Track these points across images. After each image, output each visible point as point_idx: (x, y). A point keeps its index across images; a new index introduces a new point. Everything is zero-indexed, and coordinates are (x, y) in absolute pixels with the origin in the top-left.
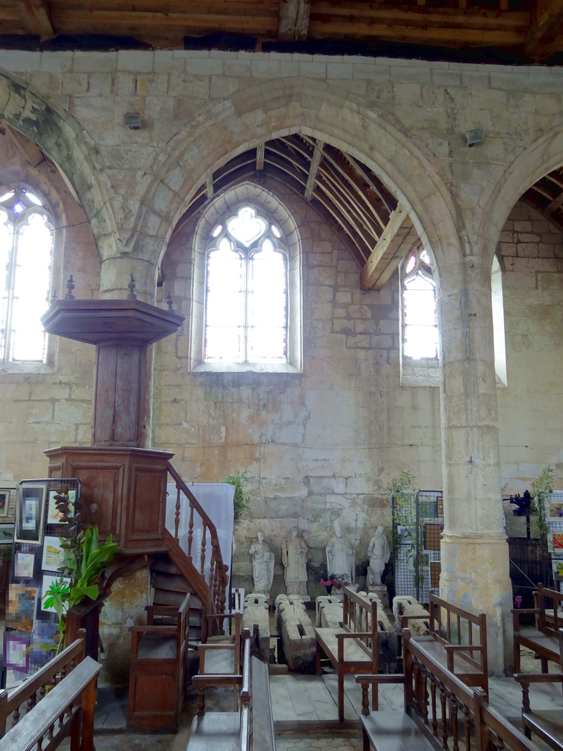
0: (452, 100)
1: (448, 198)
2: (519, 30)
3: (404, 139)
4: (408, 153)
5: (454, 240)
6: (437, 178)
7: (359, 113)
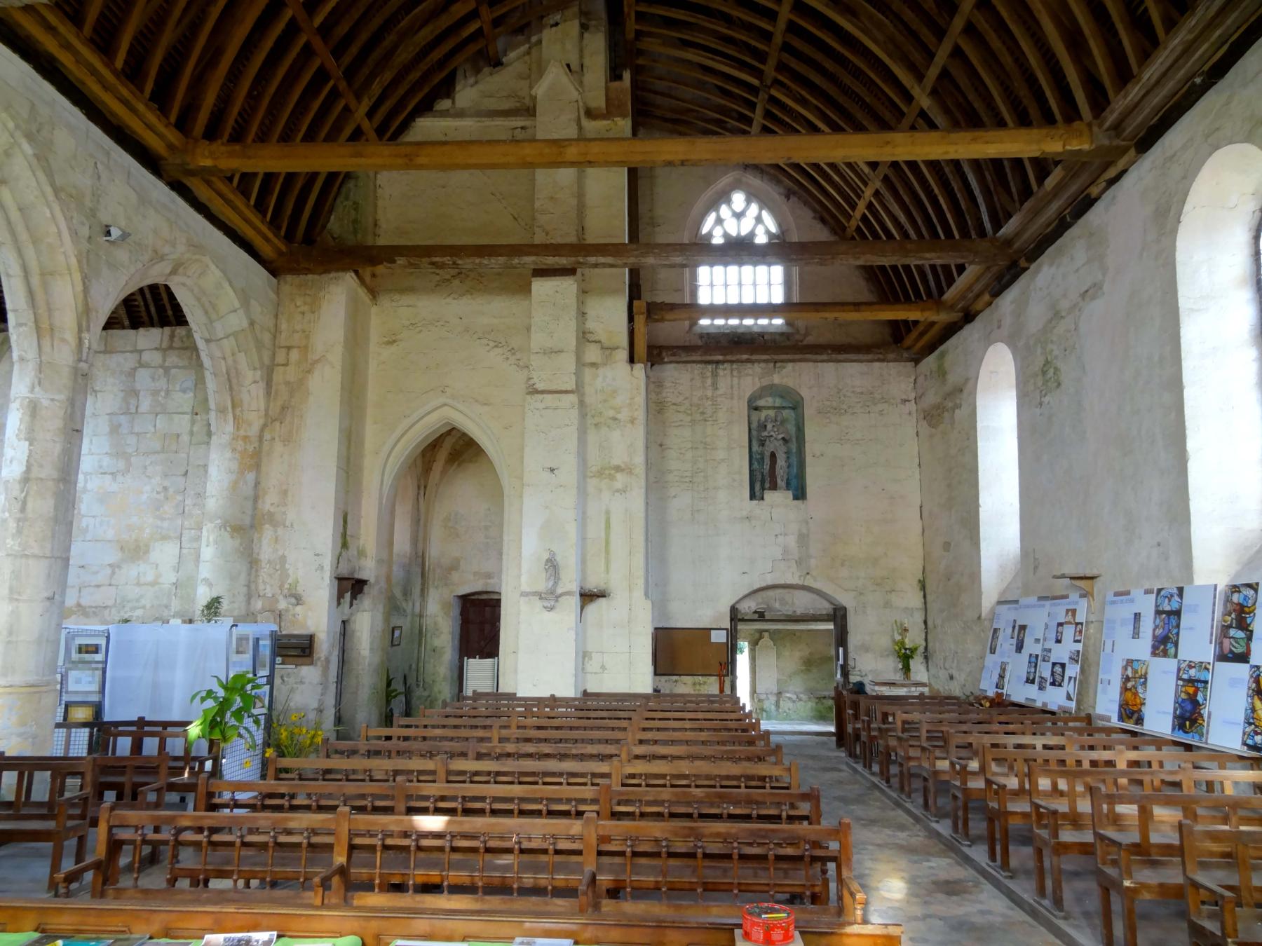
0: (99, 177)
1: (79, 288)
2: (171, 147)
3: (51, 197)
4: (48, 215)
5: (70, 337)
6: (73, 261)
7: (12, 136)
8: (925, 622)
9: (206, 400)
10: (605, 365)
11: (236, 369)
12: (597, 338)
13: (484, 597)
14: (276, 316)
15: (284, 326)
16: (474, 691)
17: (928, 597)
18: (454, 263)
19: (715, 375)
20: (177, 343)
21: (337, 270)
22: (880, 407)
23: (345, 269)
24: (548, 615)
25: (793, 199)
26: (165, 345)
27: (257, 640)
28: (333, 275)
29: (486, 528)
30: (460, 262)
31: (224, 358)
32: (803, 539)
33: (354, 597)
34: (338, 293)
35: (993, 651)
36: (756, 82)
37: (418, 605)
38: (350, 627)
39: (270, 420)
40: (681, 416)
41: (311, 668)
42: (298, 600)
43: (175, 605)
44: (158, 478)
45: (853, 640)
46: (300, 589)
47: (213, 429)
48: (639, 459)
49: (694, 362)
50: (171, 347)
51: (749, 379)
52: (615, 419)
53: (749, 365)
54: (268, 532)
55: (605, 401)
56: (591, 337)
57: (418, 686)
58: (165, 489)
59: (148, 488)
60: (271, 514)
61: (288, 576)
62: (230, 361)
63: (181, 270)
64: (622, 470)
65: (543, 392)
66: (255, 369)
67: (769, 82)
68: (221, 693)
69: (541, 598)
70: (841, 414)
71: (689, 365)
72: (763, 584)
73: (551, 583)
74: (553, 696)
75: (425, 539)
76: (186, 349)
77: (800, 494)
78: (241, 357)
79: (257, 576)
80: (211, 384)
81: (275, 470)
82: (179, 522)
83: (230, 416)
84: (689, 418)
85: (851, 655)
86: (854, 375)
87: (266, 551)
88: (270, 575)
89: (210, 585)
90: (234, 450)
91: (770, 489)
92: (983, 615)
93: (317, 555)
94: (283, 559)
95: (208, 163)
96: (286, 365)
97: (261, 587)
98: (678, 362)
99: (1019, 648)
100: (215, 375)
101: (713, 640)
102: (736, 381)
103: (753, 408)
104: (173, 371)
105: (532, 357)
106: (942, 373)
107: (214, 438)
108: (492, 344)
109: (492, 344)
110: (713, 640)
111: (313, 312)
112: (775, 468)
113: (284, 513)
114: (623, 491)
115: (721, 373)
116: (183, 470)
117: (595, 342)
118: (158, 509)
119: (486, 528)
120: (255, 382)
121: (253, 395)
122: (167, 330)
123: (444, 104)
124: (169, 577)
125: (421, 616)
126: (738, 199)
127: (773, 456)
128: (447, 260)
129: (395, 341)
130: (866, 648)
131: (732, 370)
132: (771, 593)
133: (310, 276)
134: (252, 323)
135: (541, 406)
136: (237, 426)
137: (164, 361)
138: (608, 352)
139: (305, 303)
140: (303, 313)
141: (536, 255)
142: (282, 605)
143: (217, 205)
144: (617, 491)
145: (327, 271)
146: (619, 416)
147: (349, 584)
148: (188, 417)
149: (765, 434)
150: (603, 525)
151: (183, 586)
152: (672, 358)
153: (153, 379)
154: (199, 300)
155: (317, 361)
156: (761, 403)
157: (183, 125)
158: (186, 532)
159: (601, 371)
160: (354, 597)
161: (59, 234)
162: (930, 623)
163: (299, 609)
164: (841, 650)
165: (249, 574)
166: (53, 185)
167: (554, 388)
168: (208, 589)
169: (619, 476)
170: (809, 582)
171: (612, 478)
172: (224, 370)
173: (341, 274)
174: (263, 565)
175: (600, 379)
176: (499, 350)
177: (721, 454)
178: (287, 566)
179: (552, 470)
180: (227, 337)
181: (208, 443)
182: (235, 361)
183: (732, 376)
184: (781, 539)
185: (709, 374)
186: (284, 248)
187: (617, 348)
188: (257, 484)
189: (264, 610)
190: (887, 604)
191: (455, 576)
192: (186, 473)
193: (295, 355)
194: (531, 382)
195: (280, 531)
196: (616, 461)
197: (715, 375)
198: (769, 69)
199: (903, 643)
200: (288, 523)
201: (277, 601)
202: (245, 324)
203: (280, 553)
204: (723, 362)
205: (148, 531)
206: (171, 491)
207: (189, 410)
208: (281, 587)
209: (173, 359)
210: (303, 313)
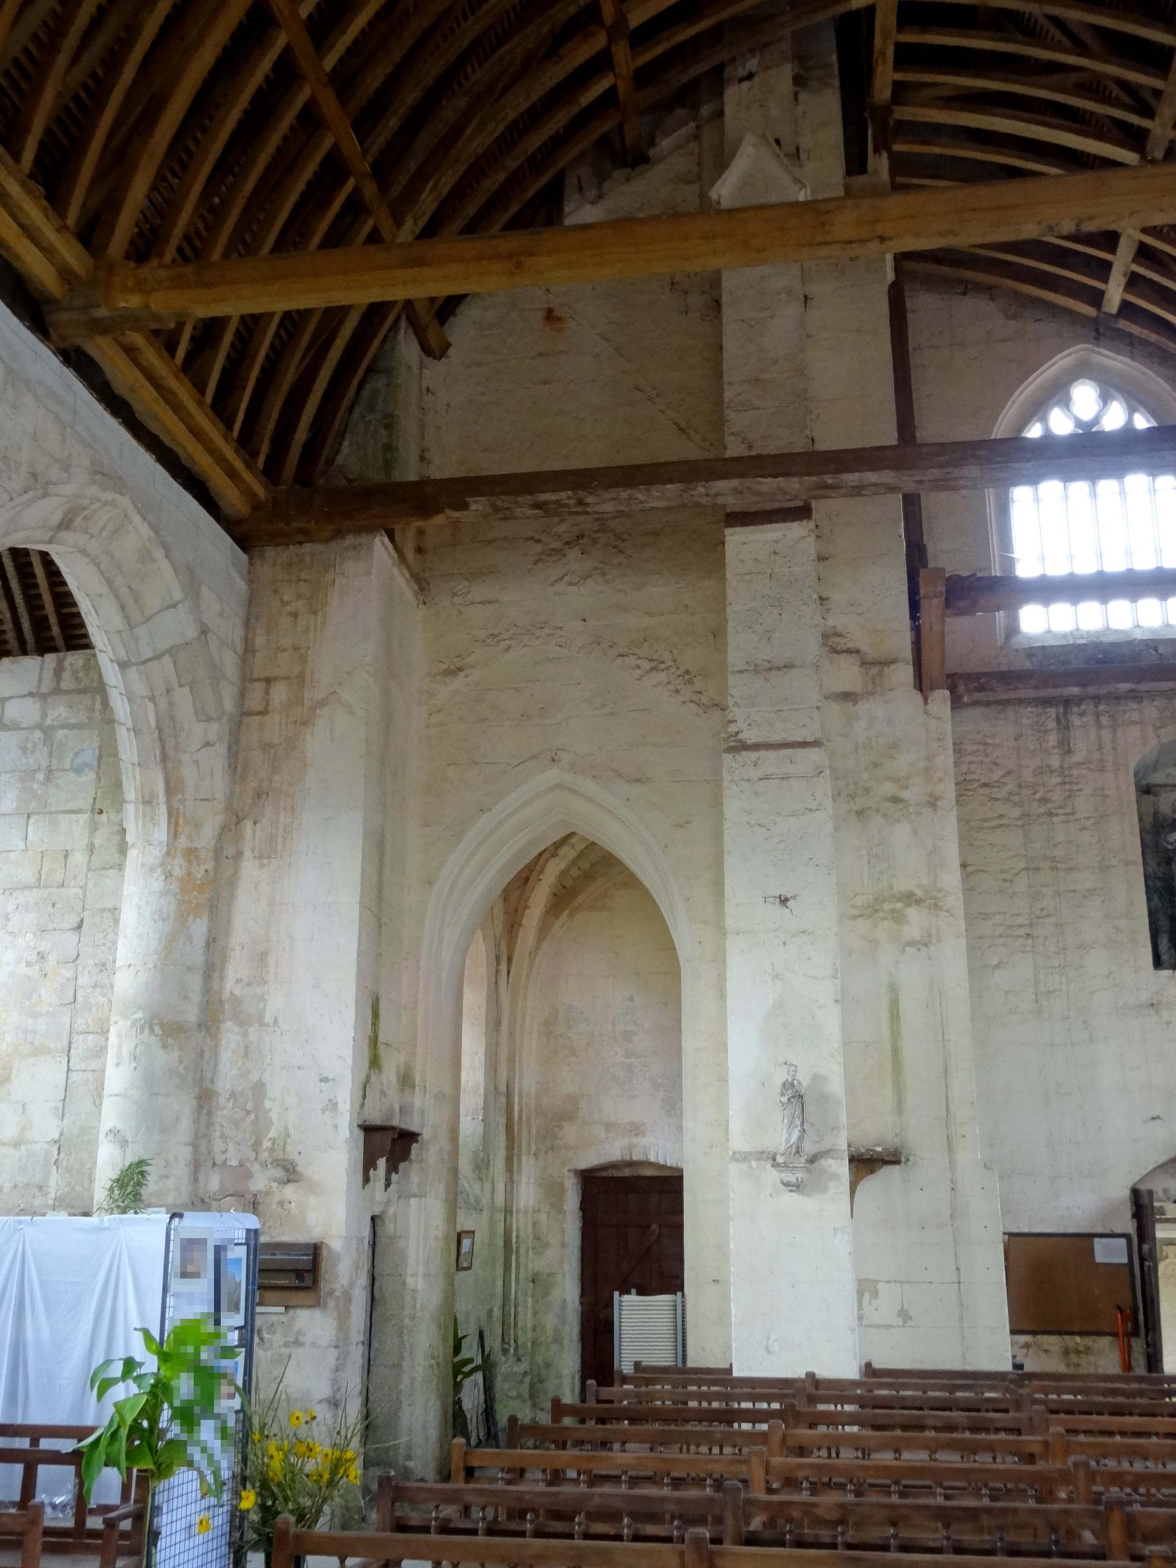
9: (119, 784)
11: (172, 718)
12: (851, 645)
13: (627, 1172)
14: (247, 624)
15: (260, 641)
16: (637, 1365)
18: (580, 502)
19: (1064, 726)
20: (67, 683)
21: (359, 531)
23: (369, 529)
26: (44, 689)
27: (219, 1250)
28: (350, 540)
29: (627, 1036)
30: (590, 499)
31: (152, 698)
33: (392, 1168)
37: (500, 1187)
38: (389, 1228)
39: (234, 820)
40: (1001, 808)
41: (316, 1313)
42: (290, 1173)
43: (56, 1183)
44: (30, 937)
46: (292, 1153)
47: (130, 838)
48: (952, 879)
49: (1021, 701)
50: (57, 691)
51: (1134, 733)
54: (231, 1037)
55: (875, 765)
56: (841, 643)
57: (505, 1351)
58: (42, 956)
59: (10, 956)
60: (236, 1001)
62: (163, 705)
63: (78, 521)
64: (919, 902)
65: (756, 747)
66: (209, 719)
68: (150, 1364)
69: (775, 1165)
71: (1010, 713)
73: (796, 1133)
74: (811, 1376)
75: (511, 1060)
76: (83, 691)
78: (183, 696)
79: (209, 1125)
80: (128, 749)
81: (247, 912)
84: (1017, 812)
87: (228, 1075)
88: (236, 1123)
90: (168, 875)
93: (324, 1080)
94: (259, 1089)
95: (133, 301)
96: (263, 713)
97: (218, 1146)
98: (988, 704)
100: (136, 731)
101: (1100, 1257)
102: (1106, 735)
103: (1146, 790)
104: (60, 734)
105: (732, 680)
107: (132, 854)
108: (646, 665)
109: (646, 665)
110: (1100, 1257)
111: (315, 613)
113: (262, 998)
114: (924, 943)
115: (1076, 721)
116: (74, 920)
117: (848, 651)
118: (28, 997)
119: (627, 1036)
120: (207, 744)
122: (50, 658)
124: (46, 1128)
125: (508, 1211)
129: (460, 669)
131: (1098, 715)
133: (308, 548)
134: (204, 631)
135: (755, 774)
136: (174, 834)
137: (44, 716)
138: (875, 670)
139: (299, 597)
141: (742, 476)
142: (260, 1182)
143: (145, 400)
144: (911, 943)
145: (338, 534)
146: (905, 794)
147: (386, 1141)
148: (83, 818)
150: (885, 1015)
151: (72, 1148)
152: (977, 696)
153: (24, 749)
154: (109, 582)
155: (322, 703)
156: (1158, 778)
157: (90, 234)
158: (78, 1040)
160: (392, 1168)
163: (289, 1191)
165: (196, 1121)
167: (776, 737)
169: (912, 912)
171: (898, 917)
172: (153, 724)
173: (364, 539)
174: (222, 1101)
175: (863, 723)
176: (662, 677)
178: (268, 1104)
179: (784, 901)
180: (157, 657)
181: (120, 867)
182: (171, 704)
183: (1099, 727)
186: (261, 492)
187: (893, 662)
188: (211, 942)
189: (224, 1194)
191: (570, 1132)
193: (279, 693)
194: (733, 728)
195: (253, 1034)
197: (1064, 726)
200: (268, 1019)
201: (249, 1175)
202: (191, 632)
203: (254, 1078)
204: (1079, 700)
205: (9, 1038)
206: (52, 960)
207: (85, 802)
208: (256, 1146)
209: (59, 711)
210: (295, 615)
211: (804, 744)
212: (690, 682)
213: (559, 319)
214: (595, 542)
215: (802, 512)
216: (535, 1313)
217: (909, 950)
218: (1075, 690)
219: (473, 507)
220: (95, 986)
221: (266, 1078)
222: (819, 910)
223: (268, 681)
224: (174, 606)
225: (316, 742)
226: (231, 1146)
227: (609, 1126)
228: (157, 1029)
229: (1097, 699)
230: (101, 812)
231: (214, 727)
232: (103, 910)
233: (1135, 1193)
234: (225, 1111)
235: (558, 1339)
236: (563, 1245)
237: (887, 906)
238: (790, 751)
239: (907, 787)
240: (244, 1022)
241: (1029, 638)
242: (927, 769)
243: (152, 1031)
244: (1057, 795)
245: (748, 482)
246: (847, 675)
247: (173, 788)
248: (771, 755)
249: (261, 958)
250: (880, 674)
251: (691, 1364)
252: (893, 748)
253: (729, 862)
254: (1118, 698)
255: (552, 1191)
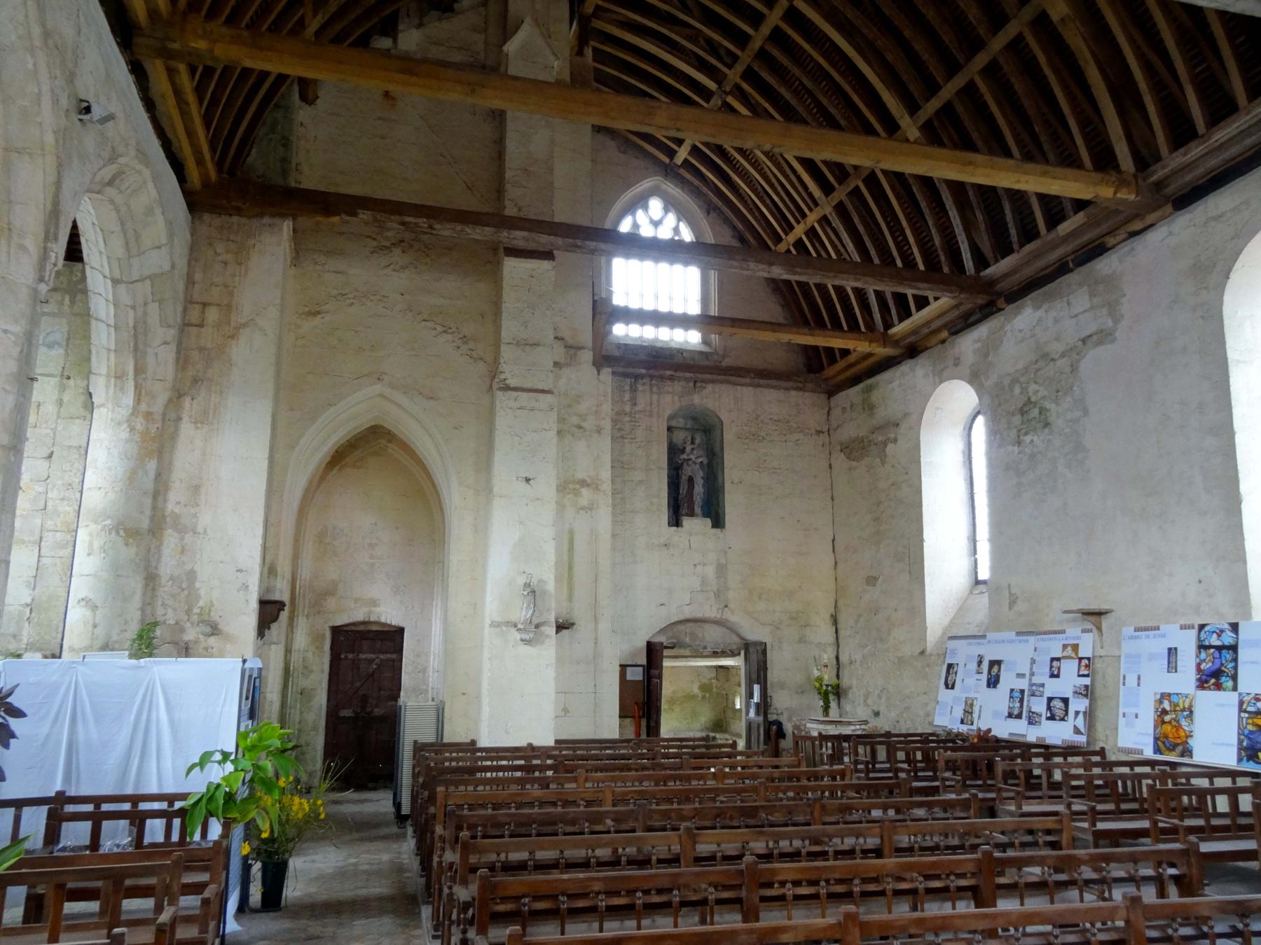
0: (79, 33)
1: (52, 178)
3: (38, 42)
4: (30, 66)
6: (49, 138)
8: (837, 658)
10: (568, 365)
11: (145, 322)
13: (361, 628)
15: (198, 276)
17: (841, 633)
18: (431, 227)
19: (633, 390)
21: (273, 215)
22: (797, 436)
24: (525, 650)
25: (713, 214)
28: (266, 220)
29: (372, 546)
30: (437, 226)
31: (133, 307)
32: (721, 569)
34: (273, 244)
35: (950, 686)
36: (712, 85)
39: (178, 395)
45: (773, 675)
46: (215, 616)
48: (606, 474)
52: (580, 427)
53: (669, 383)
54: (170, 540)
55: (569, 406)
60: (176, 517)
61: (198, 597)
62: (140, 313)
63: (117, 182)
64: (588, 485)
65: (516, 389)
66: (169, 326)
67: (728, 89)
69: (519, 630)
70: (759, 441)
72: (681, 617)
73: (531, 612)
74: (530, 745)
77: (718, 522)
78: (154, 308)
79: (153, 597)
80: (102, 337)
82: (38, 521)
83: (130, 385)
85: (770, 692)
86: (774, 403)
87: (168, 565)
88: (173, 596)
89: (94, 608)
90: (132, 429)
91: (687, 515)
92: (929, 649)
93: (240, 571)
94: (192, 576)
95: (202, 45)
96: (201, 326)
97: (160, 611)
99: (993, 682)
102: (655, 397)
103: (669, 429)
106: (870, 408)
108: (440, 329)
111: (240, 264)
112: (694, 491)
113: (195, 515)
114: (590, 508)
115: (640, 388)
116: (46, 452)
120: (165, 343)
121: (162, 359)
123: (384, 43)
126: (655, 205)
127: (691, 480)
128: (422, 222)
129: (319, 313)
130: (782, 686)
131: (651, 386)
132: (681, 627)
133: (235, 219)
136: (138, 400)
138: (572, 352)
139: (228, 252)
140: (226, 264)
141: (530, 230)
143: (168, 105)
144: (583, 508)
145: (262, 215)
146: (584, 424)
149: (685, 456)
154: (122, 224)
155: (244, 325)
156: (674, 423)
159: (566, 372)
161: (39, 95)
162: (844, 658)
164: (756, 688)
165: (144, 595)
166: (43, 25)
167: (529, 385)
168: (88, 613)
169: (584, 491)
170: (727, 615)
171: (576, 493)
172: (131, 324)
173: (277, 221)
174: (163, 581)
176: (449, 337)
177: (638, 476)
178: (197, 585)
179: (528, 480)
180: (142, 280)
182: (145, 313)
183: (652, 392)
184: (699, 568)
185: (627, 388)
186: (213, 175)
188: (158, 475)
190: (802, 640)
191: (331, 603)
192: (50, 456)
193: (212, 315)
195: (188, 538)
196: (580, 475)
197: (633, 390)
198: (733, 75)
199: (820, 679)
200: (200, 529)
201: (182, 630)
202: (167, 267)
203: (188, 567)
204: (642, 376)
208: (189, 612)
210: (226, 264)
211: (543, 391)
212: (466, 343)
213: (393, 98)
214: (411, 246)
215: (548, 255)
216: (302, 713)
217: (582, 512)
218: (643, 371)
219: (361, 216)
220: (63, 499)
221: (197, 568)
222: (546, 487)
223: (205, 305)
224: (159, 247)
225: (239, 350)
226: (170, 611)
227: (356, 600)
228: (122, 532)
229: (652, 377)
230: (69, 378)
231: (172, 332)
232: (70, 447)
233: (649, 644)
234: (166, 588)
235: (315, 728)
236: (323, 671)
237: (571, 486)
238: (535, 394)
239: (585, 420)
240: (181, 530)
241: (617, 337)
242: (596, 412)
243: (118, 533)
244: (627, 427)
245: (533, 235)
246: (559, 353)
247: (139, 370)
248: (524, 395)
249: (196, 489)
250: (575, 355)
251: (445, 741)
252: (579, 398)
253: (498, 457)
254: (662, 378)
255: (316, 638)
